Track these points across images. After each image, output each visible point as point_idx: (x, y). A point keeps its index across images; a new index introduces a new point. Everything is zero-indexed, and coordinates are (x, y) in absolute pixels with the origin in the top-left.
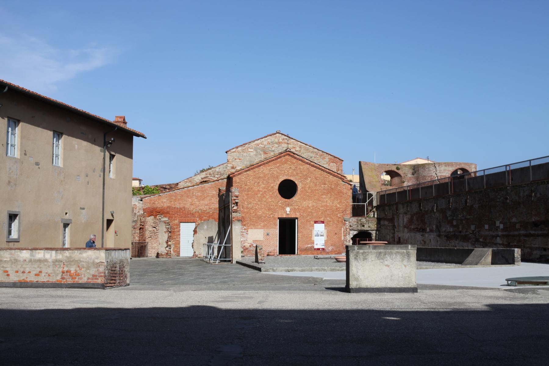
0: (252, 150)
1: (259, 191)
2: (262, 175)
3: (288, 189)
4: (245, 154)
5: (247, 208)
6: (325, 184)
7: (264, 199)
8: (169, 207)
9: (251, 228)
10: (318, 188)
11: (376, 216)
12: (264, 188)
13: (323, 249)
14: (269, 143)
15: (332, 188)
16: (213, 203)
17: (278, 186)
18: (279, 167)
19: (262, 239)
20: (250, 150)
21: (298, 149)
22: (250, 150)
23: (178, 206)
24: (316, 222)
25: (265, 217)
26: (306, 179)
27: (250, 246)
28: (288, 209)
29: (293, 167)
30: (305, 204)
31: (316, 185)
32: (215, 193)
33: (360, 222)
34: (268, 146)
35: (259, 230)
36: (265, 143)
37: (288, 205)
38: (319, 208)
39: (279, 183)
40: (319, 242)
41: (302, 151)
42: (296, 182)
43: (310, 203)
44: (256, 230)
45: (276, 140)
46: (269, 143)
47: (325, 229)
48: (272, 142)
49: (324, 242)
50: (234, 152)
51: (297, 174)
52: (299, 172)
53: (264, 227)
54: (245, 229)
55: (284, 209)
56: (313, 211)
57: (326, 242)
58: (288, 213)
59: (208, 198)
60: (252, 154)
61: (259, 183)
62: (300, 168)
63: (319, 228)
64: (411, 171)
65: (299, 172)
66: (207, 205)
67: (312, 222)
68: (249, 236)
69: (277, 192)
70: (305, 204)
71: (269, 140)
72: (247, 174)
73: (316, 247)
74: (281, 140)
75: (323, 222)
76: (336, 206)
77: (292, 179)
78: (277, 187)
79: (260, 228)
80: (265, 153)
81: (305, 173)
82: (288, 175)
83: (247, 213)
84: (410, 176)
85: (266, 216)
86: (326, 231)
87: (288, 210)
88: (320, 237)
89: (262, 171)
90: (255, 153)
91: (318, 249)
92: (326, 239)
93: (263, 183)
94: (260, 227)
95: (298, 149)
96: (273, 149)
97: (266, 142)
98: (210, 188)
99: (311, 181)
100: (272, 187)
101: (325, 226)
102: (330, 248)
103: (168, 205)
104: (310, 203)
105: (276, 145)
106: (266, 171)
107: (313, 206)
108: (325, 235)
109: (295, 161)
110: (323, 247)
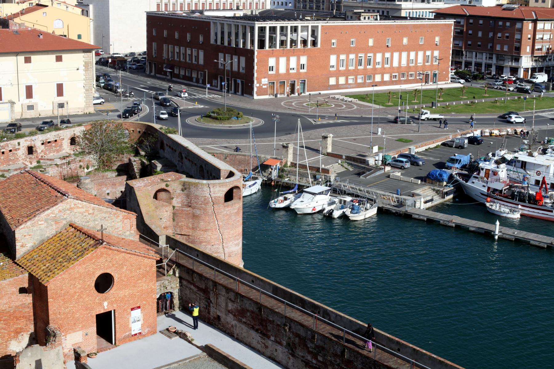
0: (42, 222)
1: (75, 292)
2: (78, 276)
3: (104, 283)
4: (35, 229)
5: (64, 313)
6: (140, 269)
7: (81, 300)
9: (70, 333)
10: (134, 274)
11: (177, 275)
12: (80, 289)
13: (140, 333)
14: (60, 211)
16: (13, 301)
18: (94, 262)
20: (40, 223)
21: (91, 211)
22: (40, 223)
24: (132, 309)
25: (82, 318)
26: (122, 268)
28: (105, 304)
29: (109, 259)
30: (121, 293)
31: (131, 272)
32: (14, 290)
33: (163, 285)
37: (105, 300)
38: (135, 295)
39: (95, 279)
40: (136, 328)
41: (96, 213)
43: (127, 292)
45: (68, 207)
46: (60, 211)
47: (141, 313)
48: (63, 210)
49: (140, 326)
50: (23, 228)
51: (113, 265)
52: (115, 262)
53: (82, 328)
55: (101, 304)
57: (143, 326)
59: (7, 297)
60: (43, 226)
61: (74, 284)
63: (137, 313)
64: (180, 187)
65: (115, 262)
66: (6, 304)
67: (129, 310)
69: (94, 289)
70: (121, 293)
71: (60, 208)
73: (133, 333)
75: (139, 307)
79: (78, 331)
80: (57, 223)
84: (179, 192)
87: (104, 304)
88: (137, 323)
89: (78, 272)
90: (46, 225)
91: (136, 335)
94: (78, 329)
95: (91, 211)
96: (65, 217)
97: (58, 210)
98: (9, 285)
102: (146, 331)
104: (127, 292)
105: (68, 212)
106: (82, 271)
108: (142, 319)
109: (110, 252)
110: (140, 331)
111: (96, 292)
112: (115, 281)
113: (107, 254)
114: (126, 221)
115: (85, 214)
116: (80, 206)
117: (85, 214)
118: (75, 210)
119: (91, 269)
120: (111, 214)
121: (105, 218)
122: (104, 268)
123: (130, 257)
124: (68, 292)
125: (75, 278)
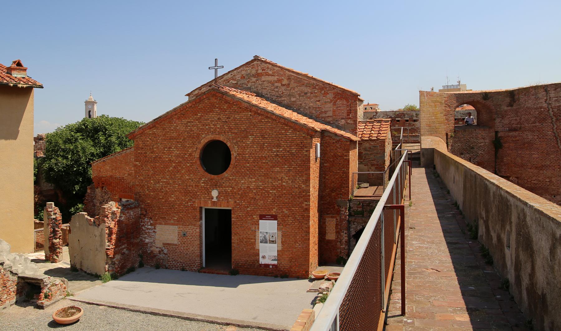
2: (175, 135)
3: (216, 157)
5: (154, 190)
6: (279, 146)
8: (111, 176)
9: (160, 224)
12: (178, 156)
15: (292, 154)
17: (199, 151)
19: (176, 242)
21: (285, 82)
23: (118, 175)
24: (262, 217)
25: (180, 205)
26: (246, 137)
27: (160, 252)
30: (243, 183)
31: (262, 148)
34: (243, 81)
35: (172, 227)
36: (238, 77)
37: (215, 186)
38: (268, 192)
39: (200, 146)
41: (293, 84)
42: (229, 144)
44: (167, 227)
45: (254, 72)
48: (247, 75)
49: (276, 254)
53: (178, 222)
54: (151, 225)
55: (209, 193)
56: (258, 197)
58: (215, 199)
61: (170, 148)
62: (235, 119)
63: (268, 227)
68: (157, 236)
69: (198, 162)
70: (243, 183)
71: (243, 72)
72: (154, 133)
74: (260, 71)
75: (274, 217)
76: (300, 187)
77: (221, 138)
78: (197, 155)
79: (173, 224)
81: (243, 127)
82: (214, 132)
83: (154, 198)
85: (181, 204)
86: (280, 233)
88: (268, 245)
92: (280, 249)
93: (176, 147)
94: (172, 222)
95: (285, 82)
96: (249, 86)
99: (253, 142)
100: (190, 155)
101: (278, 225)
103: (111, 174)
105: (254, 79)
106: (181, 128)
107: (257, 187)
108: (279, 241)
110: (276, 262)
111: (201, 170)
112: (233, 157)
113: (219, 108)
114: (339, 102)
115: (276, 84)
116: (270, 73)
117: (276, 84)
118: (263, 78)
119: (194, 129)
120: (315, 88)
121: (306, 94)
122: (215, 130)
123: (260, 121)
124: (160, 158)
125: (171, 138)
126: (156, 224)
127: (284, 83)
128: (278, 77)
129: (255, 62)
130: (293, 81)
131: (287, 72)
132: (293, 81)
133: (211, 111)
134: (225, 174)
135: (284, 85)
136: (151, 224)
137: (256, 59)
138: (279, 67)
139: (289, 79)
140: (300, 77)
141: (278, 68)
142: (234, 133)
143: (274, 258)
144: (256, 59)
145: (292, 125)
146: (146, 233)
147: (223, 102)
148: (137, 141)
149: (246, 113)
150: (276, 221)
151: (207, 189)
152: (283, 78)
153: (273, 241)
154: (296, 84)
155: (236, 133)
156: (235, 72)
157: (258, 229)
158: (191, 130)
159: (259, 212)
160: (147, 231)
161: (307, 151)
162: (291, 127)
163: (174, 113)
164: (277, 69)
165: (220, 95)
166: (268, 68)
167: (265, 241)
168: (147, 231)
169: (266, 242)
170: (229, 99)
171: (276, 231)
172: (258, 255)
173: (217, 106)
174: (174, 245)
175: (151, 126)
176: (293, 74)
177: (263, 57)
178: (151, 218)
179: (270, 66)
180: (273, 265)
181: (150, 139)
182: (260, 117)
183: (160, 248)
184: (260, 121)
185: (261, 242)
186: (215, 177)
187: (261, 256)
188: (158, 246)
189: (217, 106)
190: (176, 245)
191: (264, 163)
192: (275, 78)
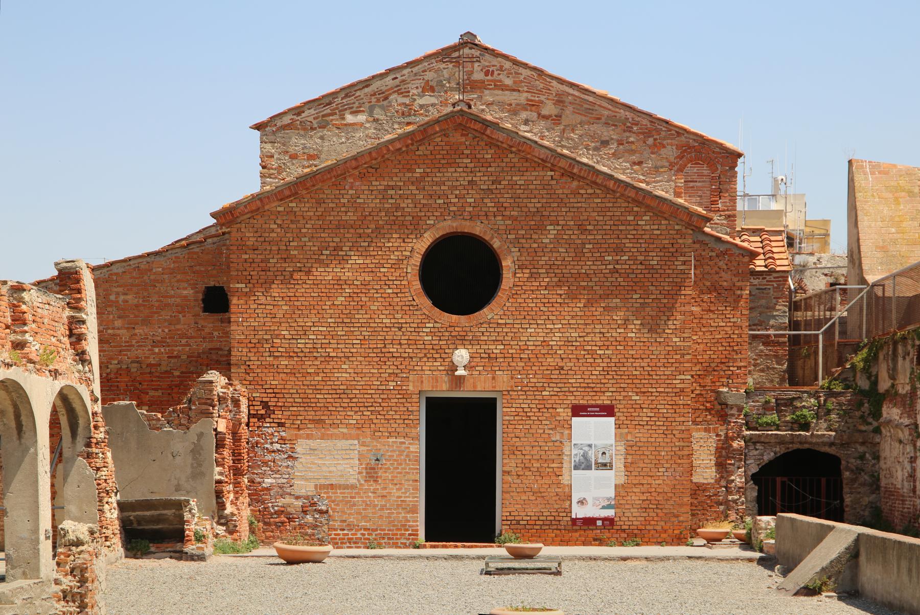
2: (351, 216)
6: (619, 250)
19: (352, 481)
21: (549, 109)
24: (578, 411)
26: (540, 228)
31: (579, 253)
37: (461, 340)
49: (611, 493)
62: (512, 185)
63: (594, 433)
71: (429, 76)
72: (291, 212)
74: (478, 76)
75: (608, 411)
77: (477, 229)
79: (345, 437)
81: (533, 205)
88: (594, 473)
92: (622, 480)
95: (549, 109)
99: (557, 240)
101: (618, 426)
108: (618, 464)
110: (610, 513)
113: (473, 157)
116: (508, 82)
119: (406, 204)
123: (575, 193)
126: (297, 437)
127: (545, 112)
128: (529, 96)
129: (467, 51)
130: (571, 108)
131: (554, 83)
132: (571, 108)
133: (450, 165)
134: (487, 313)
135: (545, 117)
136: (282, 438)
137: (468, 41)
138: (535, 69)
139: (560, 101)
140: (591, 99)
141: (529, 72)
142: (510, 217)
143: (606, 503)
144: (468, 41)
145: (654, 204)
146: (265, 463)
147: (482, 144)
148: (239, 230)
149: (541, 173)
150: (612, 420)
151: (440, 350)
152: (542, 98)
153: (605, 465)
154: (579, 118)
155: (515, 219)
156: (406, 71)
157: (570, 437)
158: (398, 208)
159: (572, 400)
160: (269, 457)
161: (684, 263)
162: (649, 208)
163: (354, 163)
164: (525, 72)
165: (478, 126)
166: (501, 68)
167: (585, 464)
168: (269, 457)
169: (589, 467)
170: (501, 136)
171: (612, 441)
172: (569, 497)
173: (467, 152)
174: (346, 487)
175: (287, 193)
176: (571, 91)
177: (483, 39)
178: (281, 425)
179: (507, 65)
180: (604, 519)
181: (280, 226)
182: (575, 183)
183: (307, 498)
184: (575, 193)
185: (576, 468)
186: (463, 319)
187: (575, 499)
188: (303, 492)
189: (467, 152)
190: (353, 487)
191: (584, 288)
192: (523, 98)
